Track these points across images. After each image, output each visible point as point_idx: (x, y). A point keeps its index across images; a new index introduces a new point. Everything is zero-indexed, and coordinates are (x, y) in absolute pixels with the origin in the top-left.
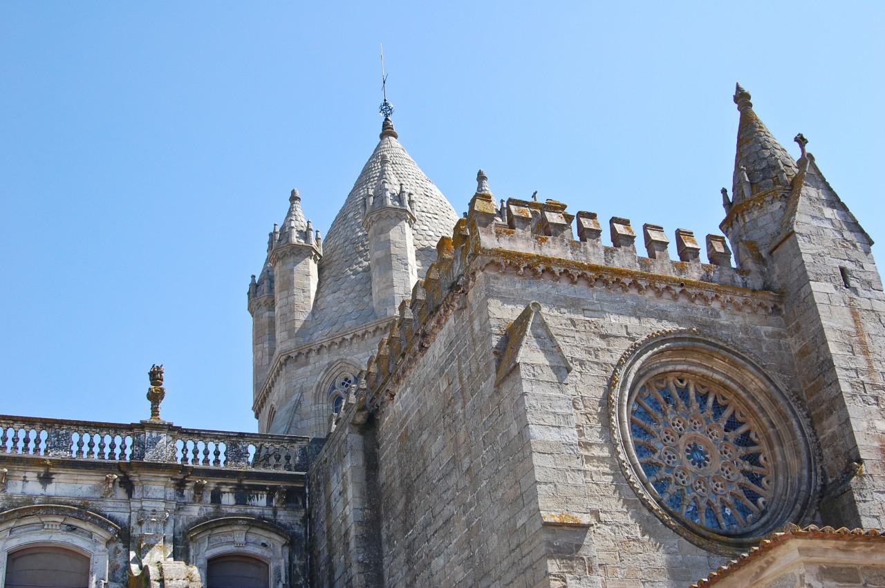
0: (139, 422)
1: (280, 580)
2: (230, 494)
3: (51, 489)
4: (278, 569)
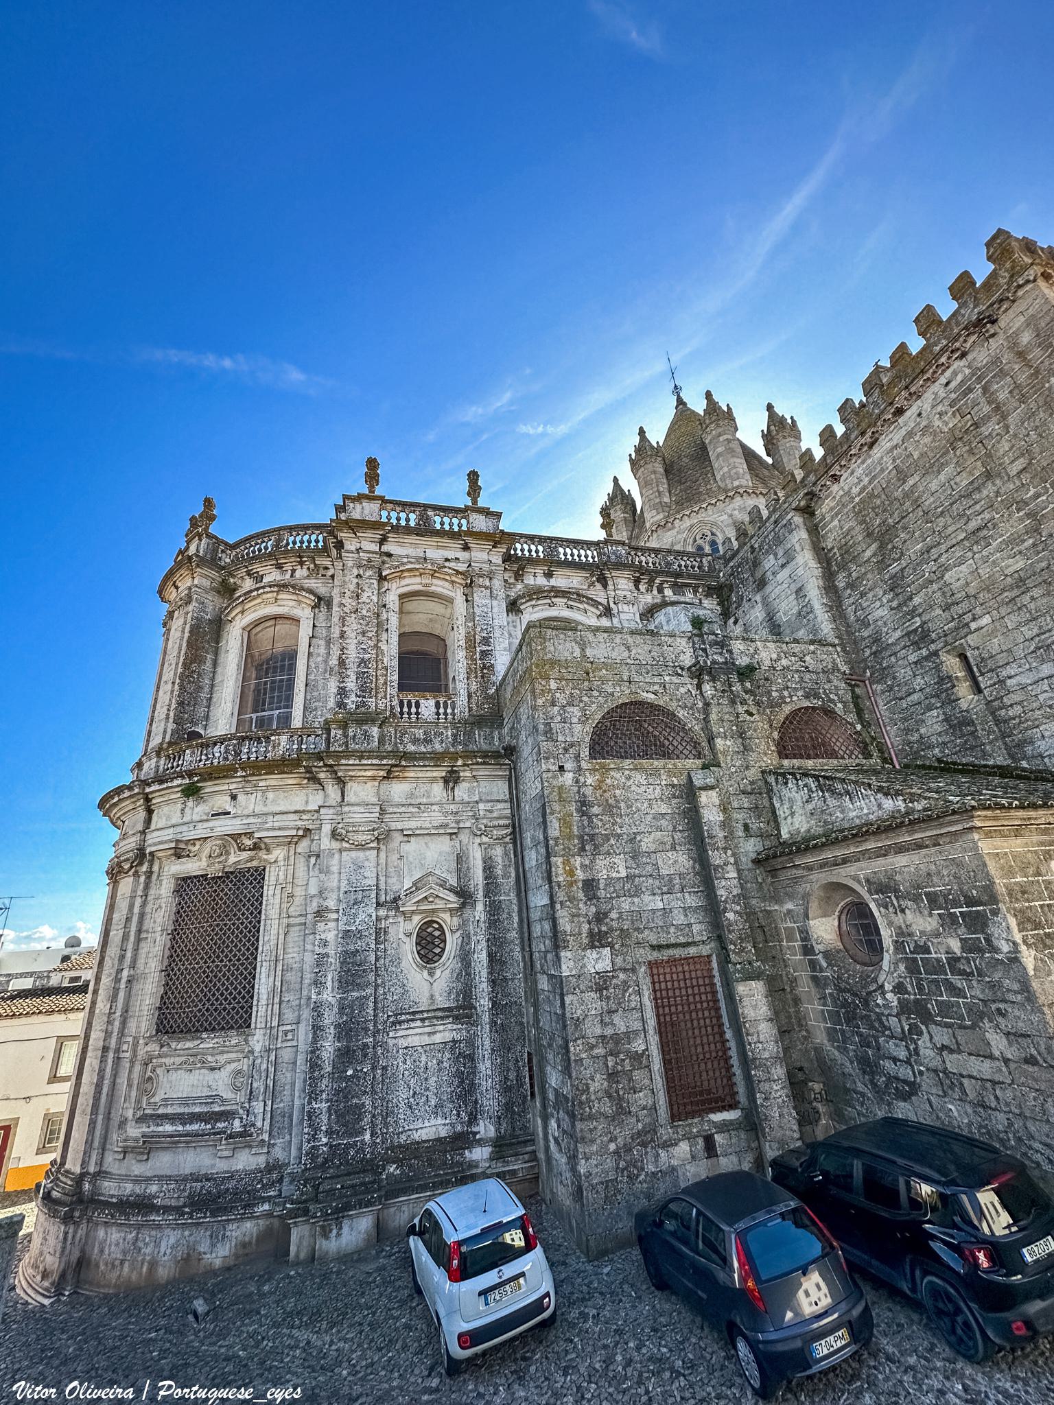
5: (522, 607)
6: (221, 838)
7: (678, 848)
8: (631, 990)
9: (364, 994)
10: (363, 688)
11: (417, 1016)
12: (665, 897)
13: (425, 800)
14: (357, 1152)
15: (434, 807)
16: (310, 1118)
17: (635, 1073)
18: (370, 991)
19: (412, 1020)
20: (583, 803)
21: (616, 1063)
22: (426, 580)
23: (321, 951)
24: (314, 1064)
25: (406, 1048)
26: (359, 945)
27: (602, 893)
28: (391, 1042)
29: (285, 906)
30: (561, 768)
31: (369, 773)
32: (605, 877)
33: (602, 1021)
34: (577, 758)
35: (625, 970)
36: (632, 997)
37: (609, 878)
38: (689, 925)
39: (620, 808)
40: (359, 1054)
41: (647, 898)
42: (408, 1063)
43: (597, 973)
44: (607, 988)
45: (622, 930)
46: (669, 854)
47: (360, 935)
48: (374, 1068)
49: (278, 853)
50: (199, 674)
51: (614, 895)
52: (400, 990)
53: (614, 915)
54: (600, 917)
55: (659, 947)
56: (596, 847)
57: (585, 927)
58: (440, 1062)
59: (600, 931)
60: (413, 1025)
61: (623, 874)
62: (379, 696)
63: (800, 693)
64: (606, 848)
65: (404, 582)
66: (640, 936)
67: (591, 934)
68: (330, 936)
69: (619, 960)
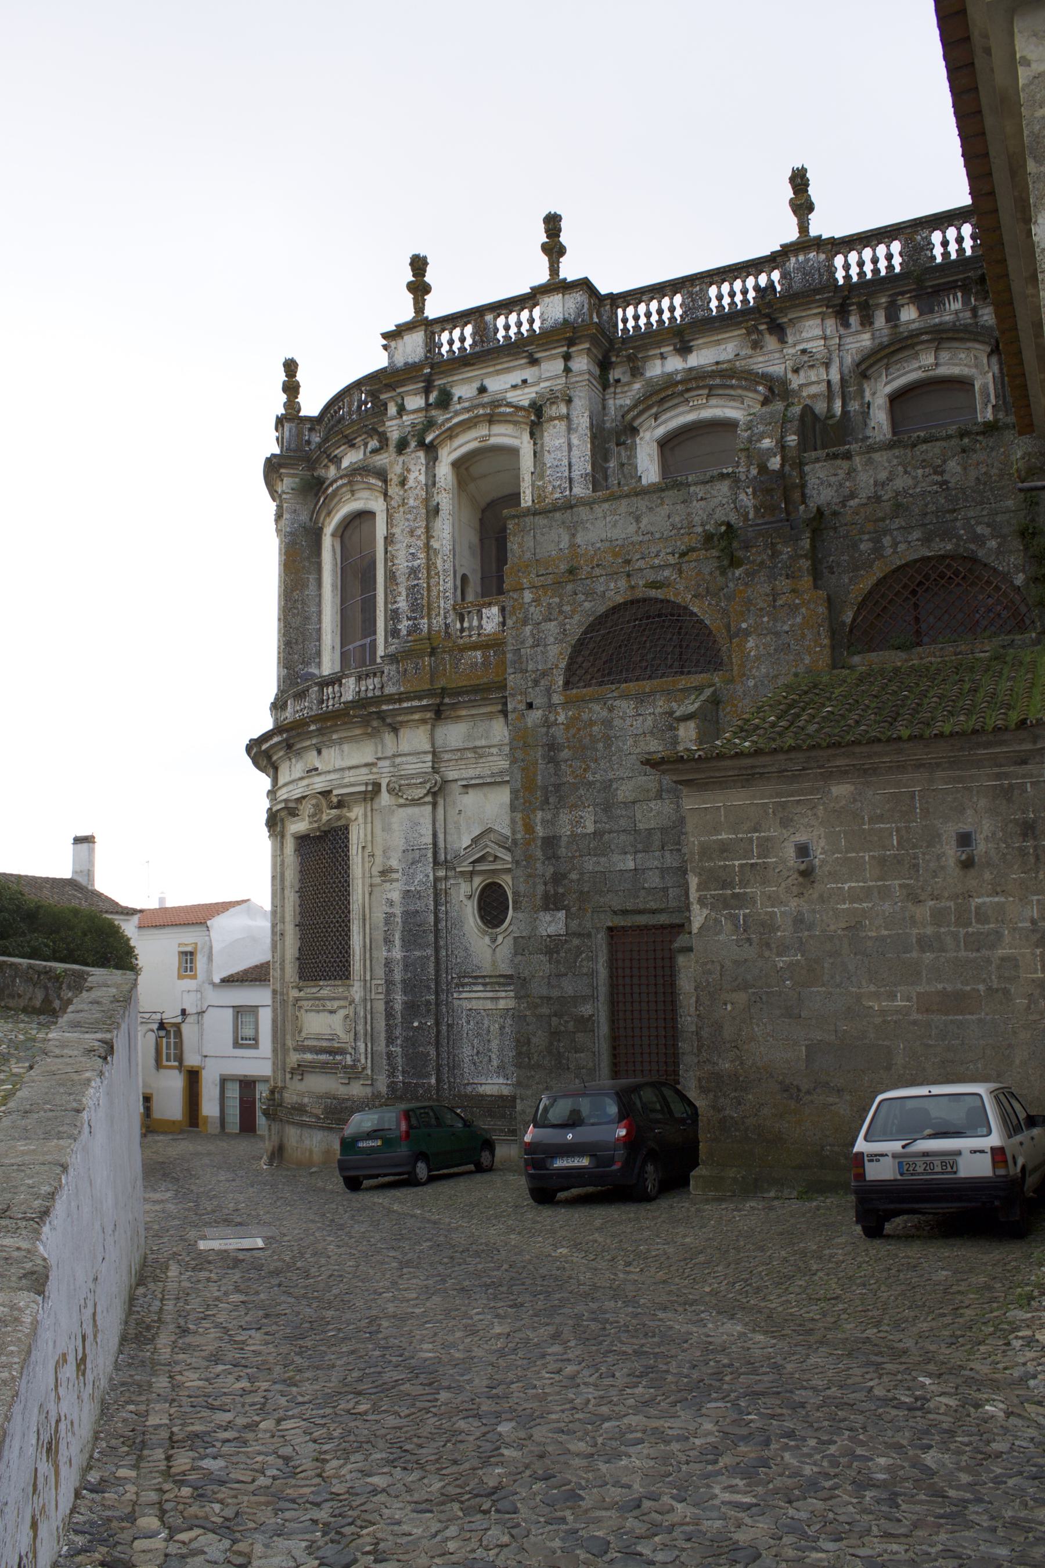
0: (779, 248)
1: (989, 401)
2: (911, 306)
3: (695, 360)
4: (985, 387)
5: (635, 424)
6: (313, 796)
7: (664, 796)
8: (584, 955)
9: (425, 954)
10: (414, 607)
11: (480, 981)
12: (640, 855)
13: (483, 743)
14: (425, 1091)
15: (494, 750)
16: (389, 1058)
17: (579, 1035)
18: (430, 951)
19: (474, 984)
20: (552, 747)
21: (560, 1024)
22: (482, 430)
23: (388, 910)
24: (389, 1014)
25: (470, 1010)
26: (419, 905)
27: (562, 851)
28: (456, 1003)
29: (367, 865)
30: (530, 706)
31: (416, 717)
32: (569, 833)
33: (549, 983)
34: (549, 692)
35: (579, 935)
36: (585, 963)
37: (574, 835)
38: (665, 889)
39: (597, 750)
40: (423, 1009)
41: (616, 858)
42: (472, 1023)
43: (549, 936)
44: (558, 952)
45: (582, 893)
46: (652, 805)
47: (418, 895)
48: (437, 1023)
49: (357, 812)
50: (303, 603)
51: (577, 854)
52: (463, 954)
53: (574, 876)
54: (558, 878)
55: (625, 912)
56: (561, 799)
57: (540, 889)
58: (502, 1028)
59: (556, 893)
60: (475, 989)
61: (590, 828)
62: (434, 613)
63: (916, 534)
64: (572, 800)
65: (457, 442)
66: (602, 900)
67: (546, 896)
68: (396, 896)
69: (574, 924)
